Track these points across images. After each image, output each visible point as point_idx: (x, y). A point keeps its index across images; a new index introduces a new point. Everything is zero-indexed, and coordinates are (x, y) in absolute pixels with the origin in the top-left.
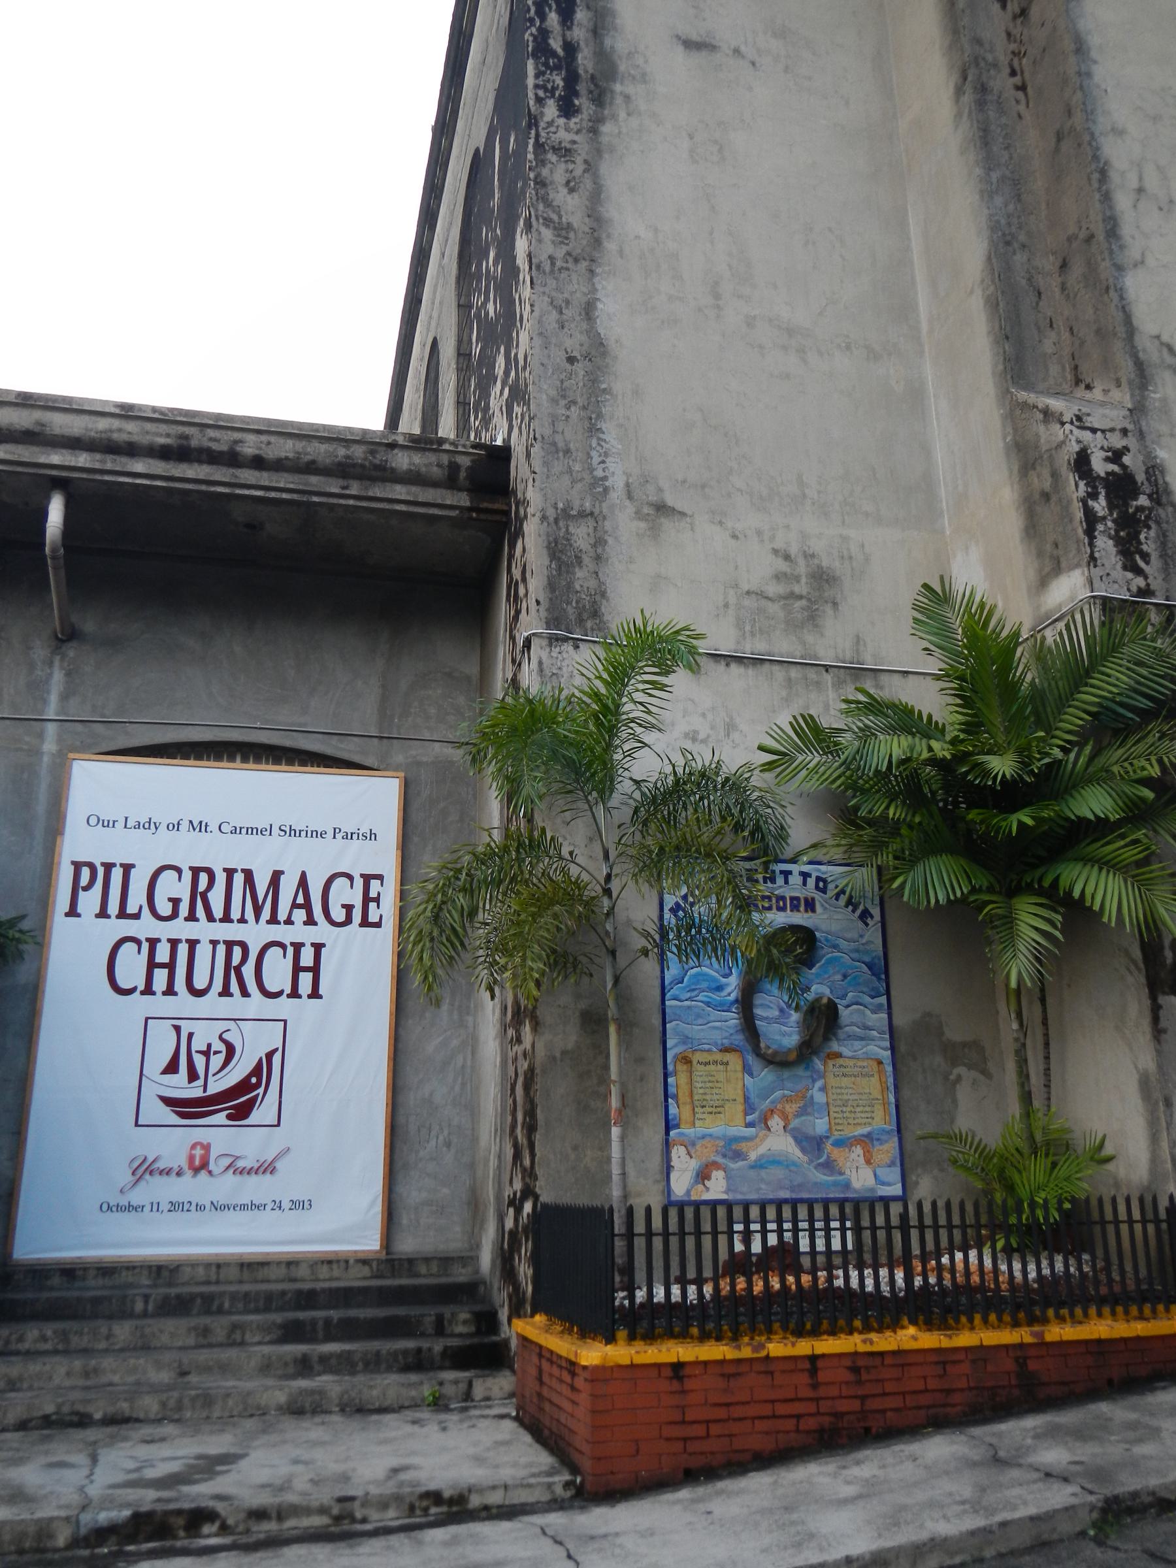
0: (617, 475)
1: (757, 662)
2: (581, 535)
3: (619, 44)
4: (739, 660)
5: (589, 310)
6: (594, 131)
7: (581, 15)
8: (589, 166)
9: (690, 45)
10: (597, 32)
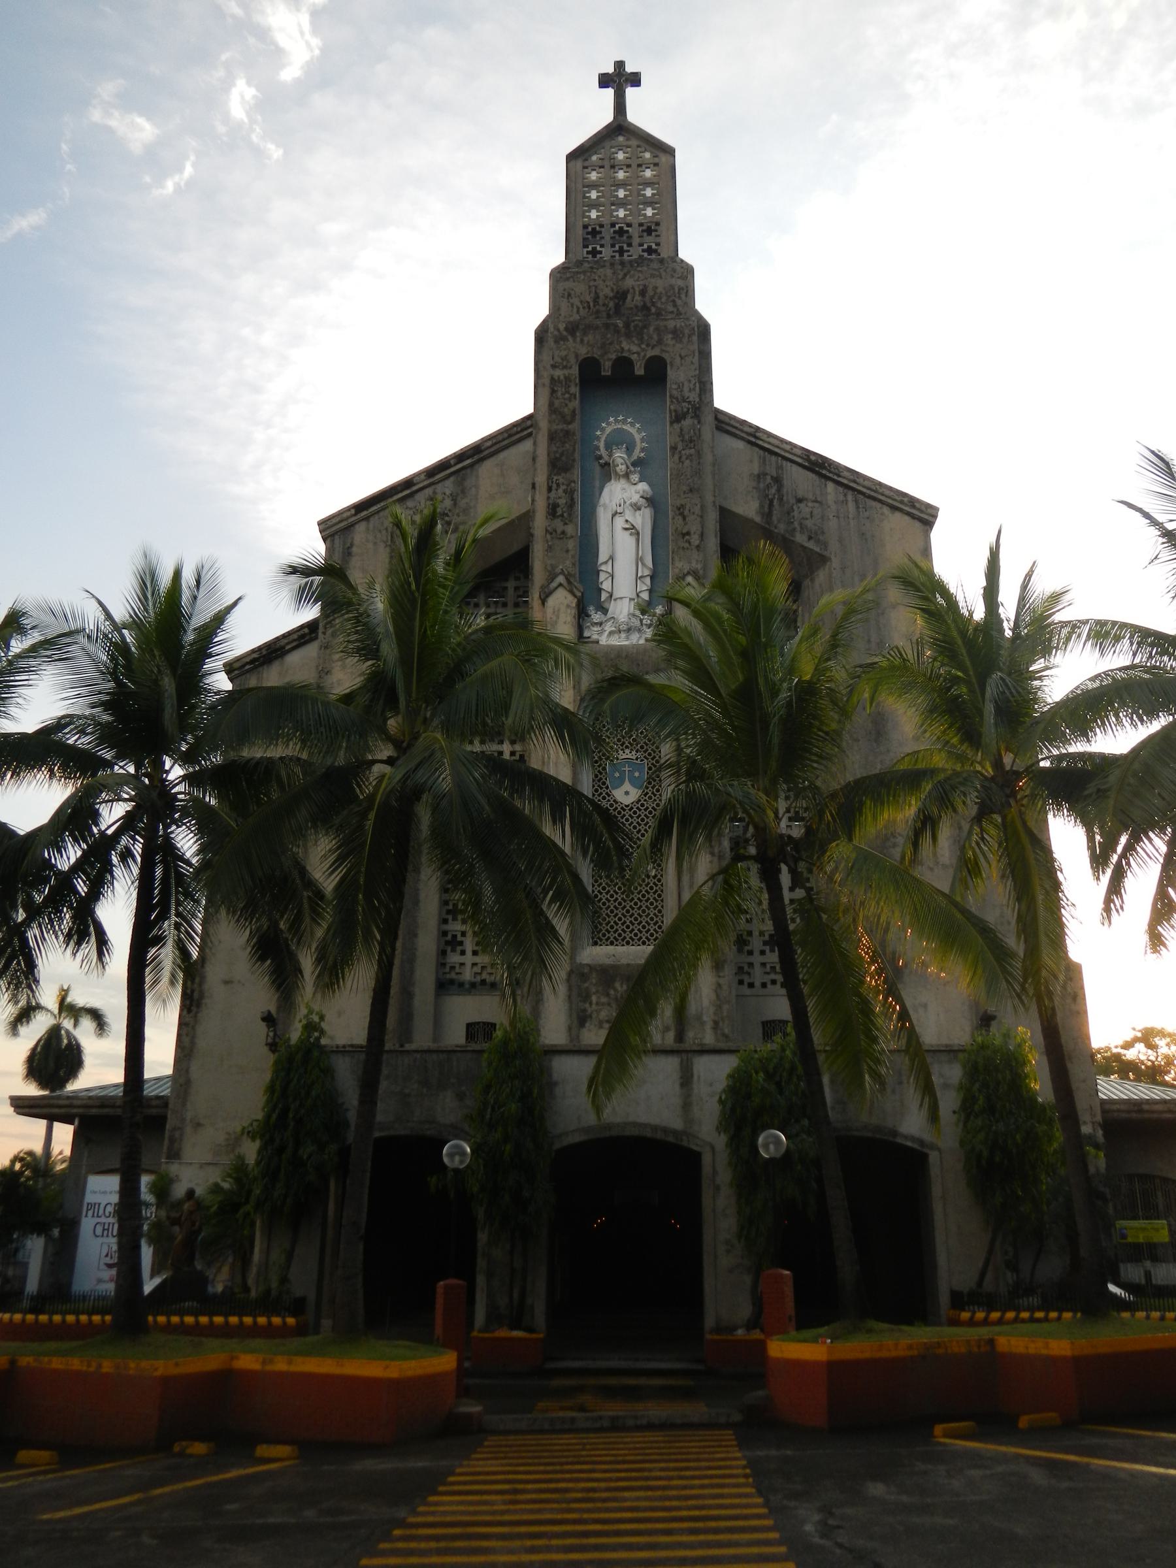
0: (189, 1116)
1: (216, 1164)
2: (177, 1134)
3: (206, 987)
4: (212, 1164)
5: (187, 1071)
6: (196, 1016)
7: (197, 980)
8: (193, 1028)
9: (227, 982)
10: (201, 984)
